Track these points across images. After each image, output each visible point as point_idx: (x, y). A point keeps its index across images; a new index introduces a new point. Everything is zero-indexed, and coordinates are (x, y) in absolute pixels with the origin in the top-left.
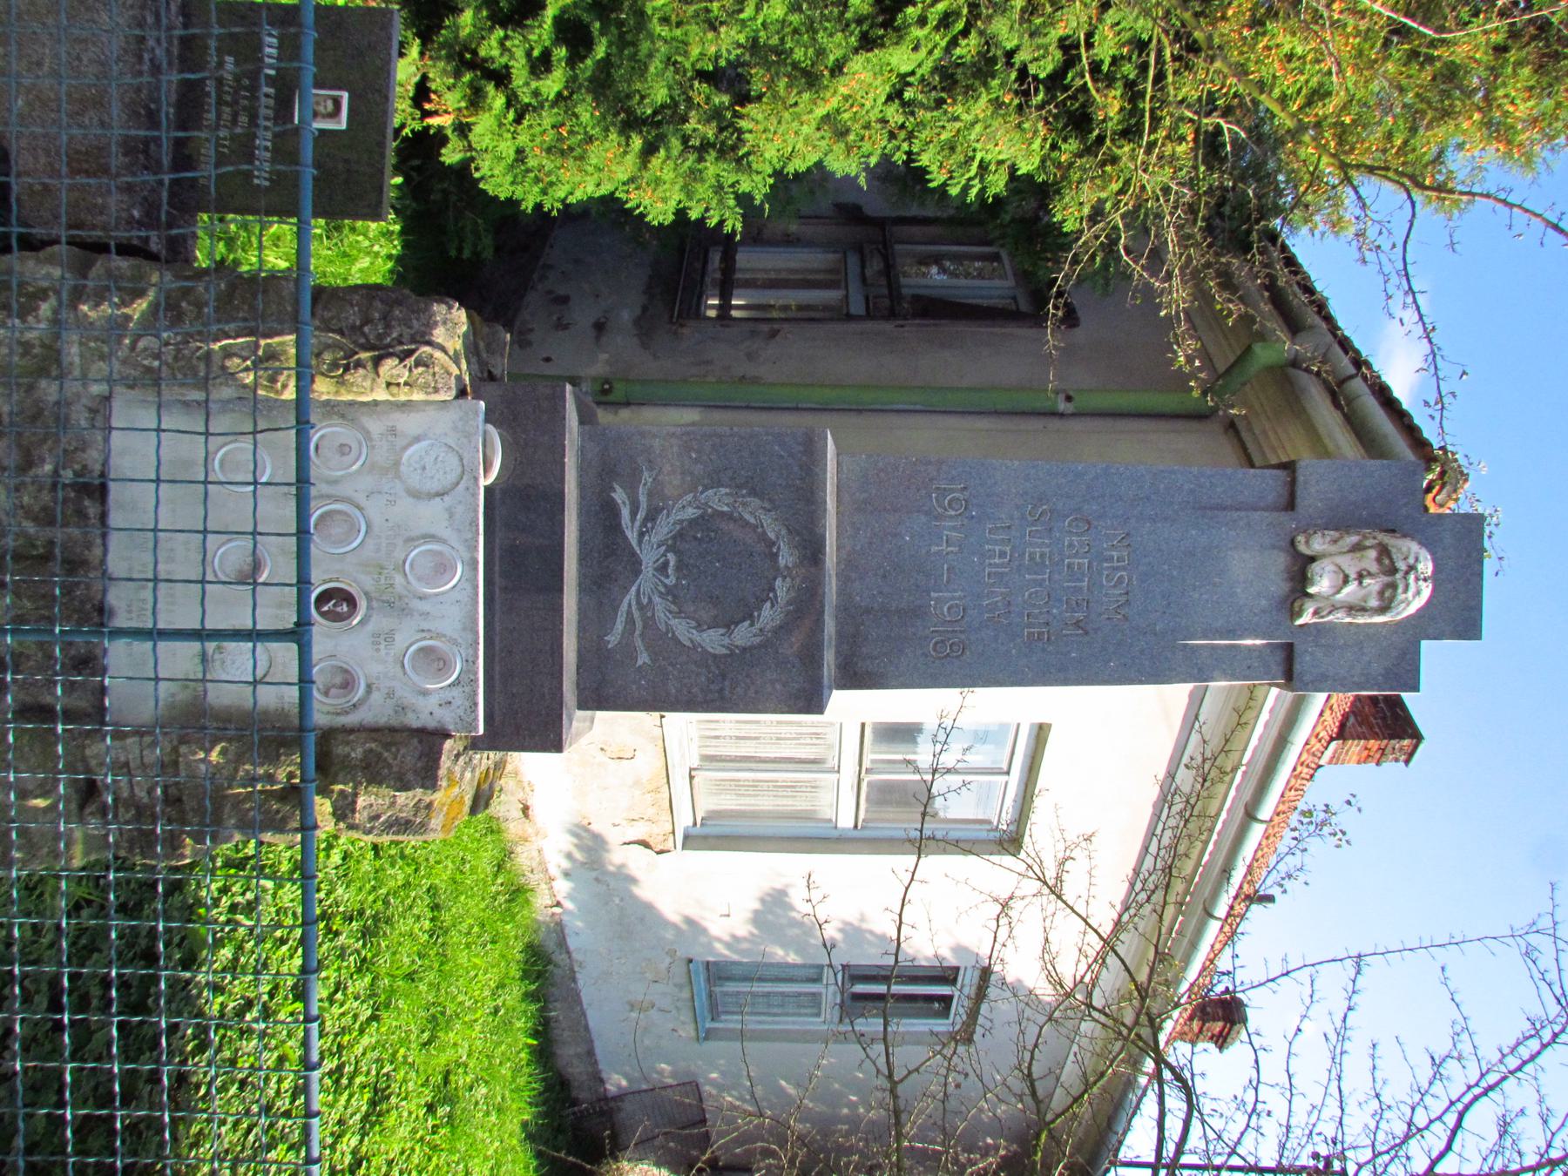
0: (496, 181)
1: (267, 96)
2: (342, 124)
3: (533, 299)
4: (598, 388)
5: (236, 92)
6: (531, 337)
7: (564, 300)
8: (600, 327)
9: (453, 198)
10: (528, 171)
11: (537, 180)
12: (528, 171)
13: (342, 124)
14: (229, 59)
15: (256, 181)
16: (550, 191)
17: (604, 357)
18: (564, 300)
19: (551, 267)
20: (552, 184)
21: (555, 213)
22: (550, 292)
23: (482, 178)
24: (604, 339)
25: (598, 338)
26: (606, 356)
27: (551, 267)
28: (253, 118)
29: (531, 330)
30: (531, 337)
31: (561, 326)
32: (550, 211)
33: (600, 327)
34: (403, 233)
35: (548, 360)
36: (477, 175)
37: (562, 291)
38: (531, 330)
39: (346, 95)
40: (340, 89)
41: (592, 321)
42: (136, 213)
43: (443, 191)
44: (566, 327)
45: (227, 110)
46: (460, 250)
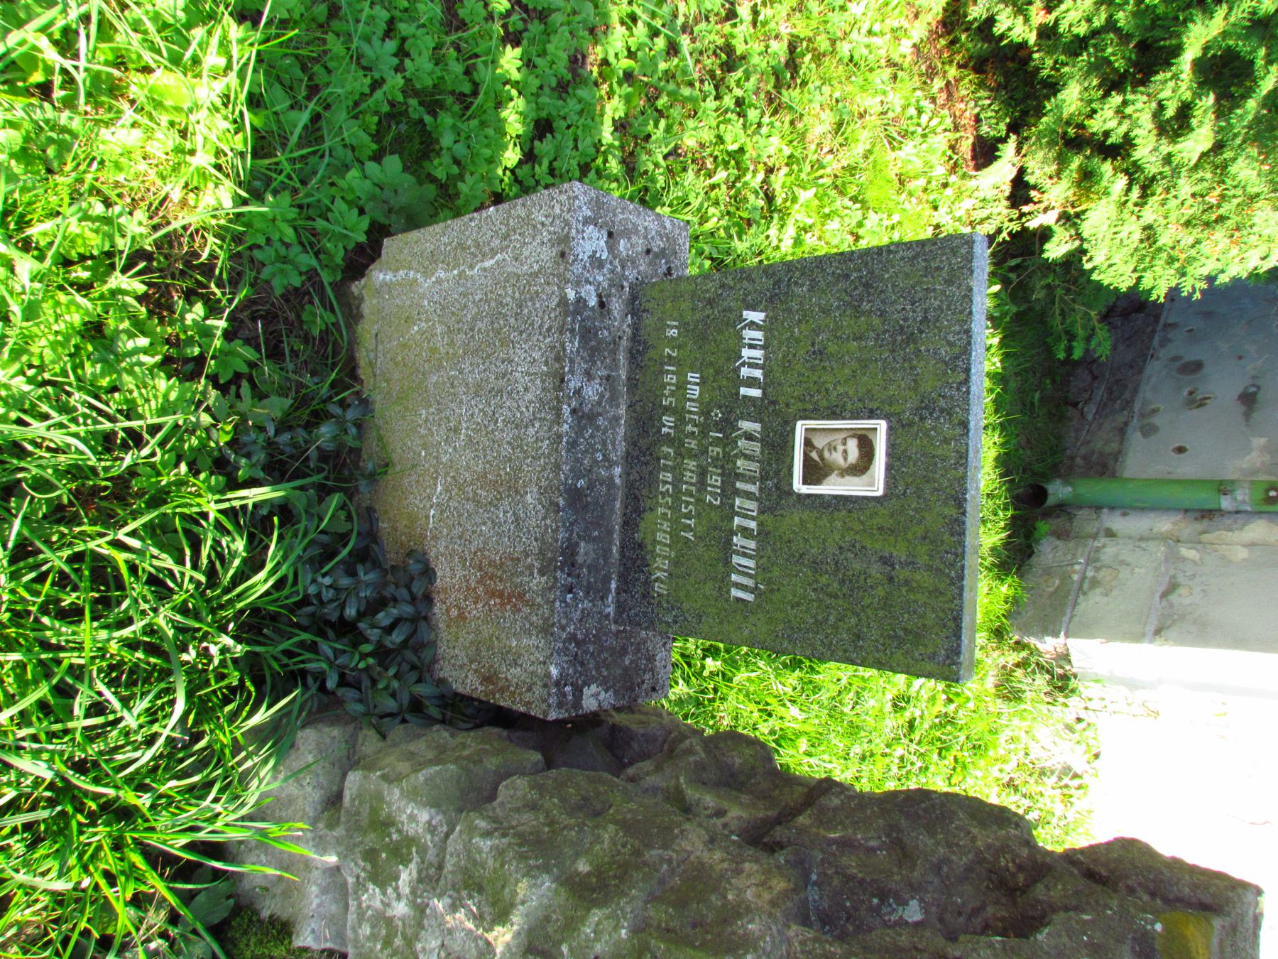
0: (1113, 266)
1: (749, 437)
2: (874, 483)
3: (1154, 369)
4: (1260, 495)
5: (704, 433)
6: (1157, 420)
7: (1198, 366)
8: (1248, 400)
9: (1059, 292)
10: (1160, 250)
11: (1171, 260)
12: (1160, 250)
13: (874, 483)
14: (693, 377)
15: (735, 593)
16: (1189, 269)
17: (1259, 442)
18: (1198, 366)
19: (1173, 326)
20: (1190, 260)
21: (1197, 296)
22: (1175, 359)
23: (1094, 268)
24: (1255, 415)
25: (1247, 415)
26: (1263, 441)
27: (1173, 326)
28: (731, 476)
29: (1155, 411)
30: (1157, 420)
31: (1196, 402)
32: (1190, 295)
33: (1248, 400)
34: (1002, 344)
35: (1181, 450)
36: (1087, 266)
37: (1191, 357)
38: (1155, 411)
39: (882, 426)
40: (872, 415)
41: (1240, 390)
42: (554, 671)
43: (1048, 287)
44: (1201, 404)
45: (692, 464)
46: (1069, 350)
